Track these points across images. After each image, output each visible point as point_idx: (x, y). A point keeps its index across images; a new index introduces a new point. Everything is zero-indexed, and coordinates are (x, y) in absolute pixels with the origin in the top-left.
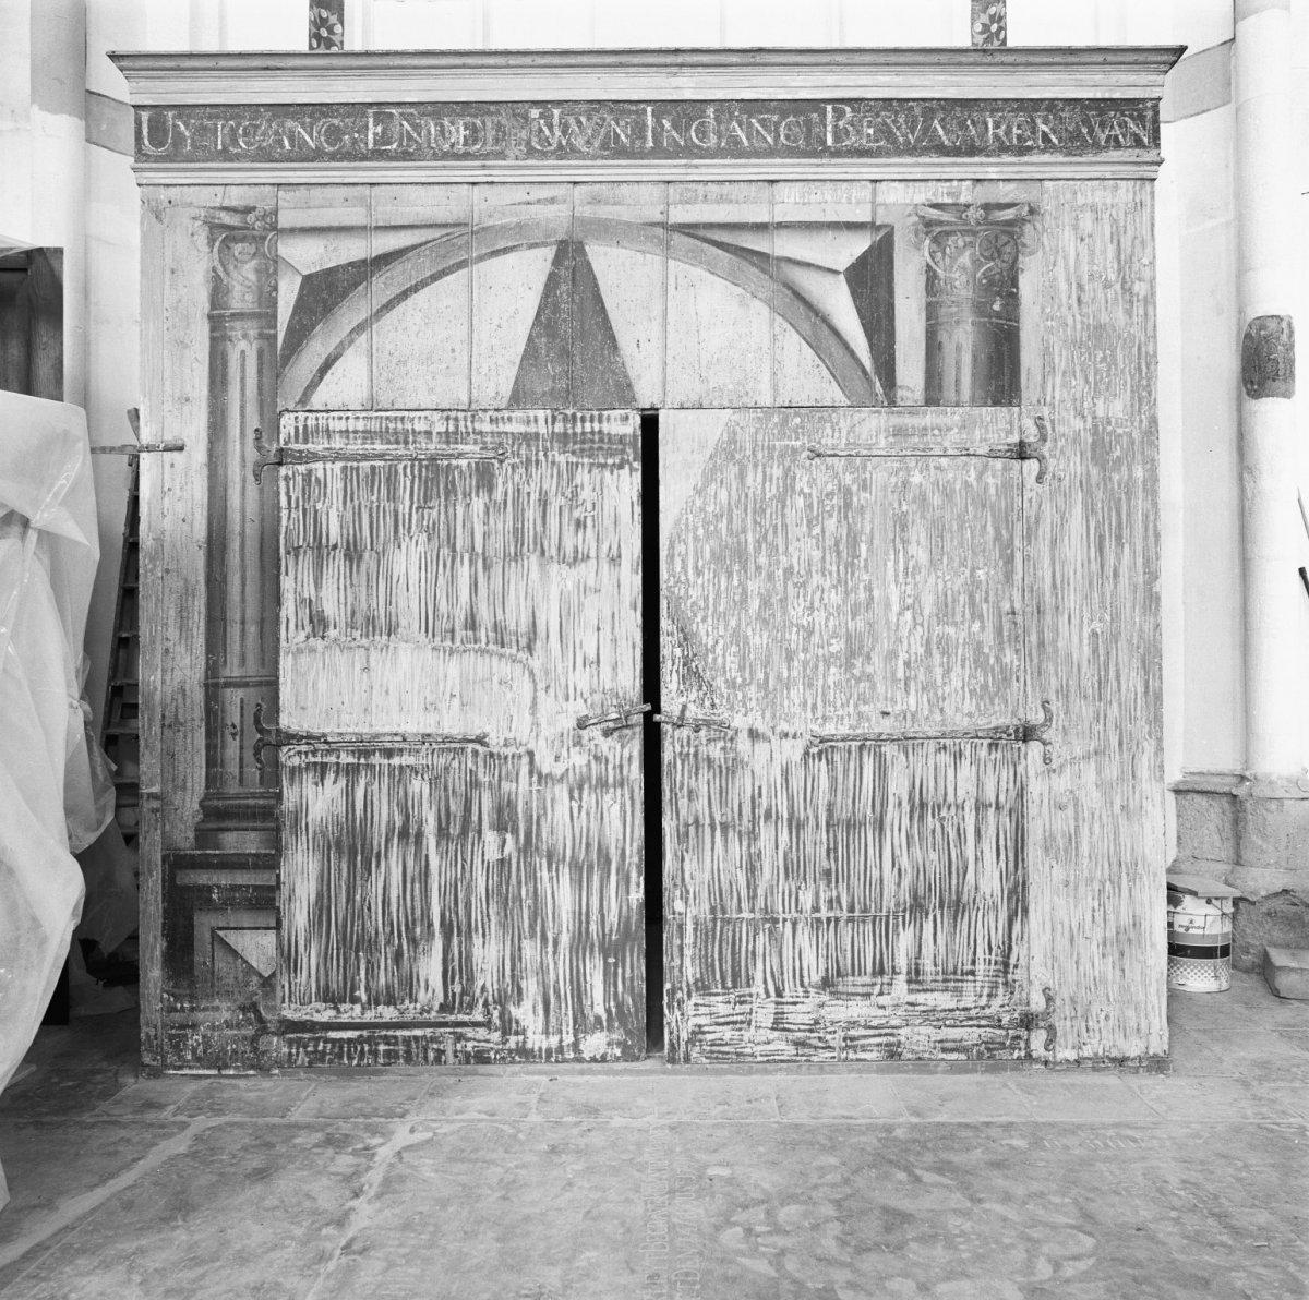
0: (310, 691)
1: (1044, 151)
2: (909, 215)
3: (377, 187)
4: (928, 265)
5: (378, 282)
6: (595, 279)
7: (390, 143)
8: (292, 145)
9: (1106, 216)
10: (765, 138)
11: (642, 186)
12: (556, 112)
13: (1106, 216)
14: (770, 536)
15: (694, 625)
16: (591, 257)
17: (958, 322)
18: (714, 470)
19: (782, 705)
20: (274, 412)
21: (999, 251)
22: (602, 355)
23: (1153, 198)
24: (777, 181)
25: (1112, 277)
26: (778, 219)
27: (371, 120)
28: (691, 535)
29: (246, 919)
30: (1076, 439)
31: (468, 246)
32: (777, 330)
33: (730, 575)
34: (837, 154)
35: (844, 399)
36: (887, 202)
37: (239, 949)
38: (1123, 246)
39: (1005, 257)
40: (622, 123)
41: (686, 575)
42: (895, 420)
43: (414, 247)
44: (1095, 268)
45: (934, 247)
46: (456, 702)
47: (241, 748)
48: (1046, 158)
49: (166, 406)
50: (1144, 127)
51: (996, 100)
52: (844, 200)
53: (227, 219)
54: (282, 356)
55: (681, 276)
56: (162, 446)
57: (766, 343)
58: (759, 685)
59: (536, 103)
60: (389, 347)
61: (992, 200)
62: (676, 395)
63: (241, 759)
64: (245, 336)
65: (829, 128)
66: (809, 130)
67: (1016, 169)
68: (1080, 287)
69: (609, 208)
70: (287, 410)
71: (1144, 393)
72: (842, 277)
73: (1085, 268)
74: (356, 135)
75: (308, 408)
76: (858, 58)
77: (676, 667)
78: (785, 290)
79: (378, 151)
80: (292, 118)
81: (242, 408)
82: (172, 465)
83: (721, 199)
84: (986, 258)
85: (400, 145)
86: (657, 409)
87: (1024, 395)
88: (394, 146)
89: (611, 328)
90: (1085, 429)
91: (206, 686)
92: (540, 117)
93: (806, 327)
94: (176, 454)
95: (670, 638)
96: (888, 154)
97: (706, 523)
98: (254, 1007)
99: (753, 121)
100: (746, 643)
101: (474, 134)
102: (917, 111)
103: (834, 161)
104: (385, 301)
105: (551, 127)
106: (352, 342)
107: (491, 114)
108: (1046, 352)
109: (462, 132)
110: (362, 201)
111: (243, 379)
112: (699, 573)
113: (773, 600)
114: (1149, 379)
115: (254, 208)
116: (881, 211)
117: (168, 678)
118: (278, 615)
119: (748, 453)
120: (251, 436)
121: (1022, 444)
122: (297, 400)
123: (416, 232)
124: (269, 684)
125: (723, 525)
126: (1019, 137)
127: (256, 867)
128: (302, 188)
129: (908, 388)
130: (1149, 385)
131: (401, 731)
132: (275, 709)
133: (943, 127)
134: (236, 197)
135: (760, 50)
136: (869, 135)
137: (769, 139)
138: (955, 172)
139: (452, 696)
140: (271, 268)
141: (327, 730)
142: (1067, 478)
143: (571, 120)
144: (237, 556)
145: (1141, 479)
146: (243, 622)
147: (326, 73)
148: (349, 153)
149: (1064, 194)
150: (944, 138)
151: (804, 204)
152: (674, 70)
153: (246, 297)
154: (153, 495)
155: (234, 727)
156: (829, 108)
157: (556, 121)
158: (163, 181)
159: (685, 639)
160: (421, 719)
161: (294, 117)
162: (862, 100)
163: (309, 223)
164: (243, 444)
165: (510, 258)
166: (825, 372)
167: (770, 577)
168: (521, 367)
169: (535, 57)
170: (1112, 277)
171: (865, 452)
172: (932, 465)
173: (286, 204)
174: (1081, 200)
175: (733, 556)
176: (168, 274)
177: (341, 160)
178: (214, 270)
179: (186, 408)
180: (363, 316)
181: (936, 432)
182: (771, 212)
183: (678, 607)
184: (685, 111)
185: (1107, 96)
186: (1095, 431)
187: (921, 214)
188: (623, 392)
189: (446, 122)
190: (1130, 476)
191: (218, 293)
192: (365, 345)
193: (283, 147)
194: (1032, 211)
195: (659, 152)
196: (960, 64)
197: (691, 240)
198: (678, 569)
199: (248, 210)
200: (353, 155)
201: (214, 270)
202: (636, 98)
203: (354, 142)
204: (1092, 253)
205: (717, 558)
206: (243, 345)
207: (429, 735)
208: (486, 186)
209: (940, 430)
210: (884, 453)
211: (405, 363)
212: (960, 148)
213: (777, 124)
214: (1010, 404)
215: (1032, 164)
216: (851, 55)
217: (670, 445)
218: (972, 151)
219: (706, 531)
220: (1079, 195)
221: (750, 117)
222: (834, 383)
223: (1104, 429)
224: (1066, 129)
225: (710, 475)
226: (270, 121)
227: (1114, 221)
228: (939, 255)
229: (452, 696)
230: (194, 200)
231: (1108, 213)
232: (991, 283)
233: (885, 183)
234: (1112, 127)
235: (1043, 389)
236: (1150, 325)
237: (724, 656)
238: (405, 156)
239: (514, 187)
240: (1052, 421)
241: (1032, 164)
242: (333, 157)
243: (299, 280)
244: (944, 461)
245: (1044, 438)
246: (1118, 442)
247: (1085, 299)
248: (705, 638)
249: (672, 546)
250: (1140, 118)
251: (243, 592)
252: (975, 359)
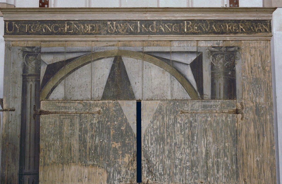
0: (47, 176)
1: (241, 33)
2: (207, 49)
3: (67, 42)
4: (212, 63)
5: (67, 67)
6: (124, 66)
7: (71, 30)
8: (45, 31)
9: (258, 50)
10: (169, 30)
11: (137, 42)
12: (114, 23)
13: (258, 50)
14: (171, 134)
15: (151, 158)
16: (123, 60)
17: (220, 78)
18: (156, 116)
19: (174, 180)
20: (40, 101)
21: (230, 59)
22: (126, 86)
23: (270, 45)
24: (172, 41)
25: (260, 66)
26: (172, 50)
27: (66, 25)
28: (150, 134)
30: (251, 108)
31: (91, 58)
32: (172, 80)
33: (160, 145)
34: (187, 34)
35: (190, 98)
36: (201, 46)
38: (262, 57)
39: (232, 60)
40: (132, 26)
41: (148, 145)
42: (203, 103)
43: (77, 57)
44: (255, 63)
45: (213, 58)
46: (87, 179)
48: (242, 35)
49: (10, 99)
50: (267, 27)
51: (229, 20)
52: (190, 46)
53: (27, 50)
54: (41, 86)
55: (147, 65)
56: (9, 109)
57: (169, 84)
58: (168, 175)
59: (109, 21)
60: (70, 84)
61: (228, 45)
62: (146, 96)
64: (32, 81)
65: (185, 27)
66: (180, 28)
67: (234, 38)
68: (252, 68)
69: (128, 48)
70: (42, 100)
71: (269, 96)
72: (189, 66)
73: (253, 63)
74: (62, 28)
75: (48, 100)
76: (192, 10)
77: (146, 170)
78: (174, 69)
79: (68, 32)
80: (45, 24)
81: (31, 99)
82: (12, 115)
83: (158, 45)
84: (227, 61)
85: (74, 31)
86: (141, 100)
87: (237, 96)
88: (72, 31)
89: (129, 79)
90: (254, 106)
91: (19, 175)
92: (110, 24)
93: (180, 79)
94: (13, 112)
95: (144, 162)
96: (201, 34)
97: (154, 131)
99: (166, 25)
100: (164, 163)
101: (93, 28)
102: (208, 23)
103: (186, 36)
104: (69, 71)
105: (113, 27)
106: (60, 82)
107: (97, 23)
108: (243, 85)
109: (90, 28)
110: (63, 45)
111: (31, 92)
112: (152, 144)
113: (172, 152)
114: (270, 92)
115: (35, 47)
116: (199, 48)
117: (9, 172)
118: (39, 155)
119: (165, 112)
120: (33, 107)
121: (237, 110)
122: (45, 97)
123: (78, 53)
125: (158, 131)
126: (235, 29)
128: (48, 42)
129: (207, 95)
130: (270, 94)
133: (215, 27)
134: (30, 44)
135: (168, 8)
136: (196, 29)
137: (170, 30)
138: (219, 38)
139: (86, 177)
140: (39, 63)
142: (249, 119)
143: (118, 25)
144: (28, 139)
145: (269, 119)
146: (30, 157)
147: (55, 13)
148: (60, 33)
149: (247, 44)
150: (215, 30)
151: (179, 46)
152: (145, 12)
153: (32, 70)
154: (6, 123)
156: (185, 22)
157: (114, 25)
158: (11, 40)
159: (148, 162)
161: (46, 23)
162: (194, 20)
163: (49, 51)
164: (30, 109)
165: (102, 61)
166: (185, 91)
167: (171, 145)
168: (105, 89)
169: (109, 9)
170: (260, 66)
171: (195, 112)
172: (213, 115)
173: (43, 46)
174: (251, 45)
175: (160, 140)
176: (12, 64)
177: (58, 35)
178: (24, 63)
179: (16, 99)
180: (63, 75)
181: (214, 106)
182: (170, 49)
183: (146, 153)
184: (148, 23)
185: (257, 19)
186: (256, 107)
187: (210, 49)
188: (131, 96)
189: (86, 25)
190: (266, 118)
191: (25, 69)
192: (63, 83)
193: (43, 31)
194: (239, 48)
195: (141, 33)
196: (219, 11)
197: (150, 56)
198: (146, 143)
199: (33, 47)
200: (61, 33)
201: (24, 63)
202: (135, 19)
203: (62, 30)
204: (254, 59)
205: (156, 140)
206: (31, 83)
208: (96, 42)
209: (215, 106)
210: (200, 112)
211: (74, 88)
212: (219, 32)
213: (172, 26)
214: (234, 99)
215: (238, 36)
216: (191, 9)
217: (144, 110)
218: (223, 33)
219: (154, 133)
220: (251, 44)
221: (165, 24)
222: (187, 94)
223: (259, 106)
224: (247, 27)
225: (155, 118)
226: (40, 25)
227: (260, 51)
228: (214, 60)
229: (86, 177)
230: (19, 45)
231: (259, 49)
232: (228, 67)
233: (200, 41)
234: (259, 27)
235: (242, 95)
236: (270, 78)
237: (158, 167)
238: (75, 34)
239: (103, 42)
240: (245, 104)
241: (238, 36)
242: (56, 34)
243: (46, 66)
244: (216, 114)
245: (243, 108)
246: (262, 109)
247: (253, 71)
248: (153, 162)
249: (145, 137)
250: (266, 25)
251: (30, 149)
252: (224, 87)
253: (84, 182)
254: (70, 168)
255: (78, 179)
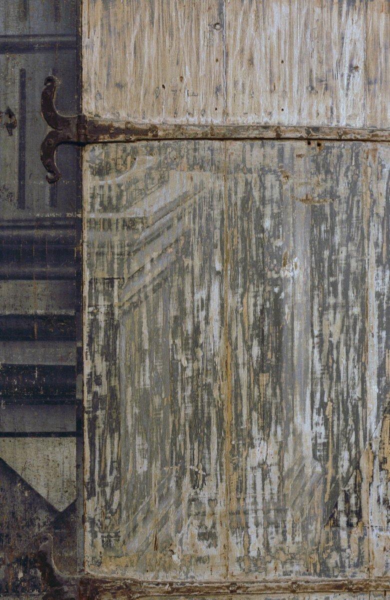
29: (29, 419)
37: (18, 467)
46: (358, 78)
47: (22, 148)
63: (22, 165)
98: (42, 560)
124: (64, 46)
127: (46, 337)
131: (273, 121)
132: (76, 86)
139: (353, 68)
141: (156, 121)
155: (10, 114)
160: (305, 106)
207: (316, 129)
253: (341, 93)
254: (264, 15)
255: (311, 80)
